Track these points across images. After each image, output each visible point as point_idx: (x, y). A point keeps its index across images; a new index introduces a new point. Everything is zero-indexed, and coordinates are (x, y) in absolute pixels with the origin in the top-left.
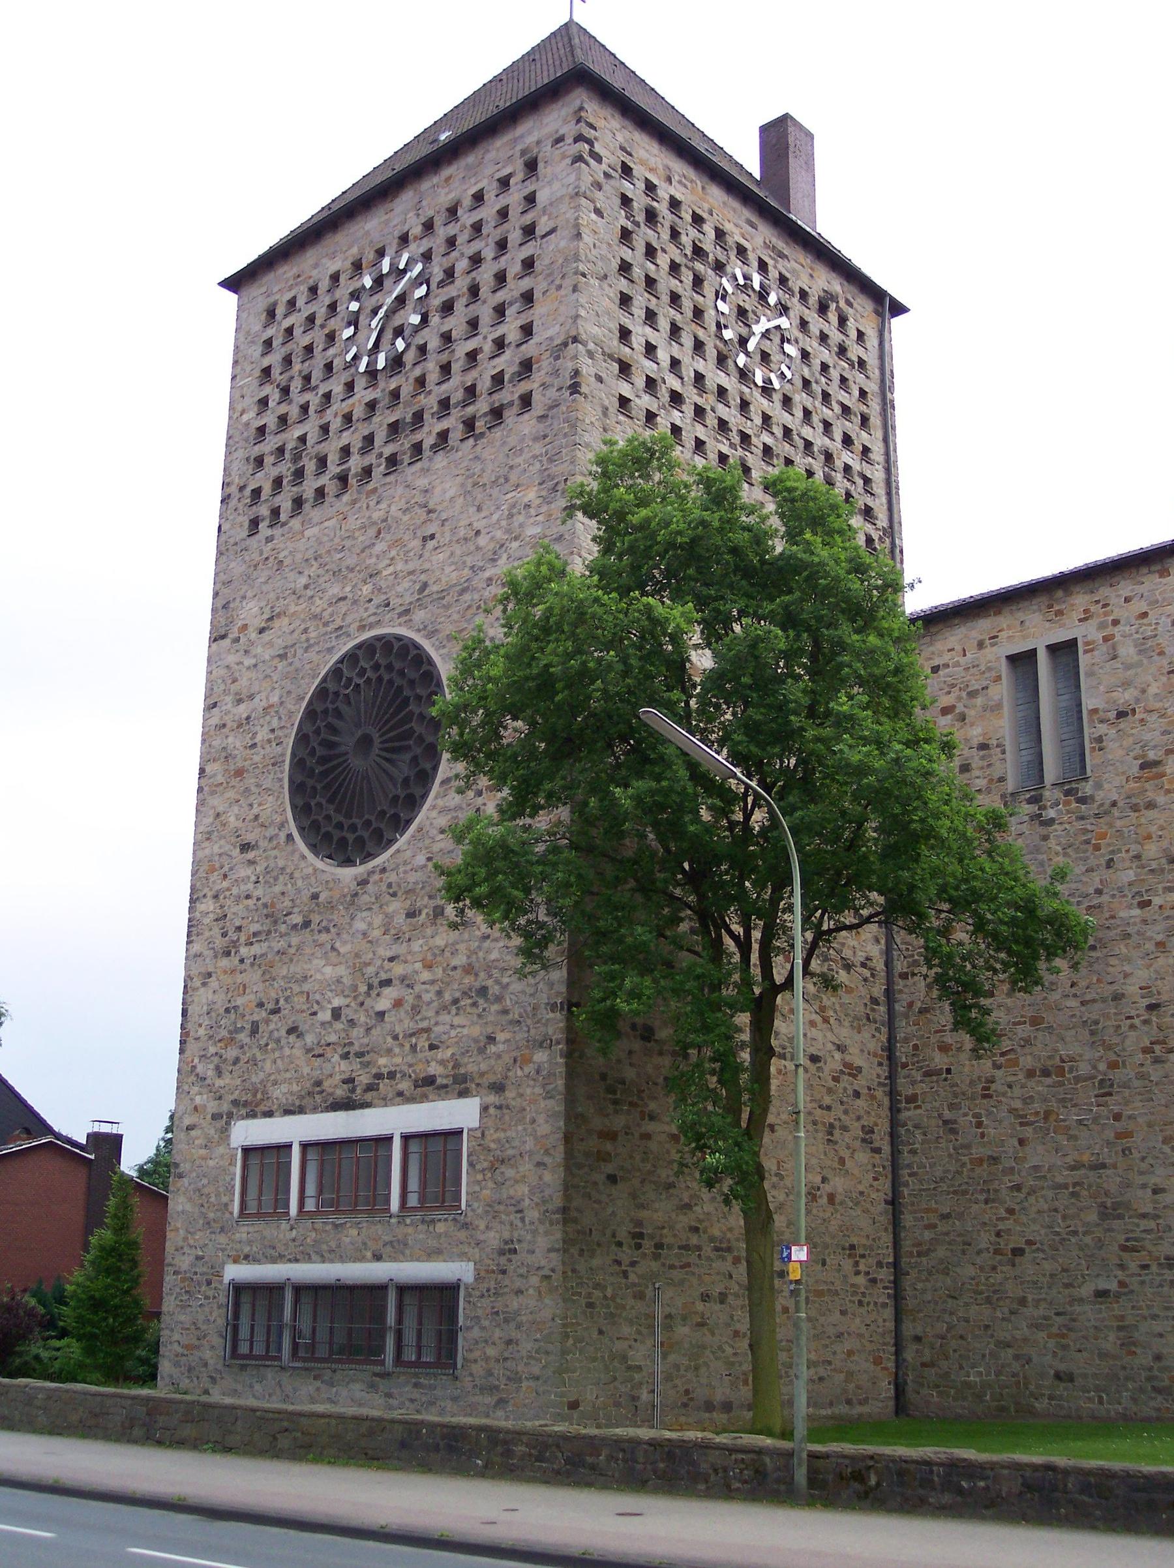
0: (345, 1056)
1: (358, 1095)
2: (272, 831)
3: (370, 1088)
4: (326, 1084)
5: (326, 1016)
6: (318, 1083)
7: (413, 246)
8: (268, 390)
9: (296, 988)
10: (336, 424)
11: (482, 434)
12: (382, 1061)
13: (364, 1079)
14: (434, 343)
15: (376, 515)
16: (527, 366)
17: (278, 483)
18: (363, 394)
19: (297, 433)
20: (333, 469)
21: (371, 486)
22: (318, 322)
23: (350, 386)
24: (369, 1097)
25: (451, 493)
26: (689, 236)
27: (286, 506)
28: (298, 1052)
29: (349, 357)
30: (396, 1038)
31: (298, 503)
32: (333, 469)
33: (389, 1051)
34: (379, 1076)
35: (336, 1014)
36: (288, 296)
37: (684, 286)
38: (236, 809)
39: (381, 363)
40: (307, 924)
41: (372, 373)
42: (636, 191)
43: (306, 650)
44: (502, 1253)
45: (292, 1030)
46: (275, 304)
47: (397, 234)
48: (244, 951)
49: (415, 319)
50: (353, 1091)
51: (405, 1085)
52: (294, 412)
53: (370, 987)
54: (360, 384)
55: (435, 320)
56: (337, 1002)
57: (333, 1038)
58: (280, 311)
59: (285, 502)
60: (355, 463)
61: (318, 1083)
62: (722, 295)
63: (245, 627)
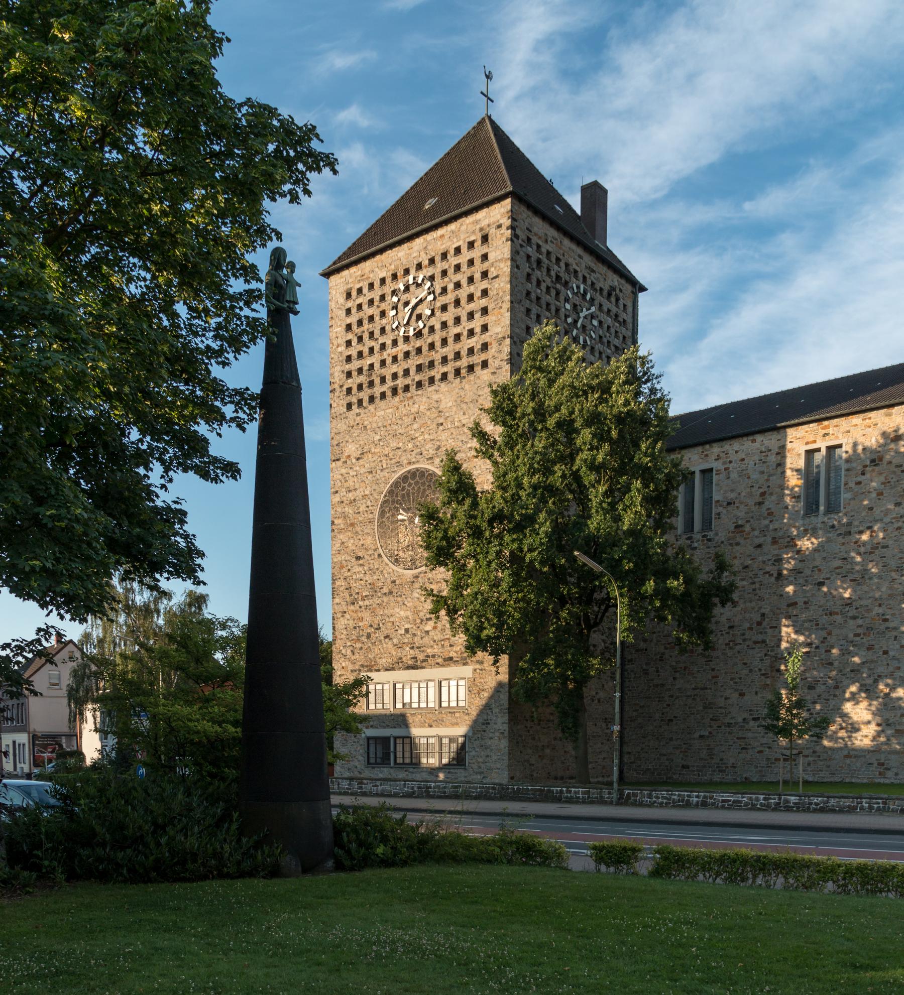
0: (412, 648)
1: (419, 663)
2: (370, 552)
3: (424, 661)
4: (404, 659)
5: (403, 632)
7: (425, 271)
8: (350, 336)
9: (387, 620)
10: (389, 361)
11: (464, 377)
12: (429, 651)
13: (421, 657)
14: (438, 327)
15: (414, 409)
16: (485, 347)
17: (360, 387)
18: (402, 347)
19: (369, 362)
20: (390, 383)
21: (409, 395)
22: (376, 303)
23: (395, 343)
24: (424, 664)
25: (450, 404)
27: (366, 399)
29: (394, 327)
30: (435, 641)
31: (372, 399)
32: (390, 383)
33: (432, 647)
34: (428, 656)
35: (407, 631)
36: (358, 286)
38: (352, 541)
39: (411, 333)
40: (391, 593)
41: (407, 339)
43: (382, 470)
44: (483, 724)
46: (351, 289)
47: (416, 263)
48: (361, 603)
49: (428, 312)
50: (417, 662)
52: (366, 351)
53: (422, 620)
54: (400, 341)
55: (438, 313)
56: (407, 626)
57: (406, 641)
58: (354, 293)
59: (364, 395)
60: (401, 382)
63: (349, 456)
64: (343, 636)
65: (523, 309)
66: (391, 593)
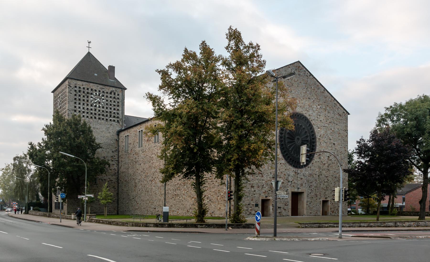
26: (86, 91)
37: (86, 98)
42: (77, 89)
62: (92, 97)
65: (74, 103)
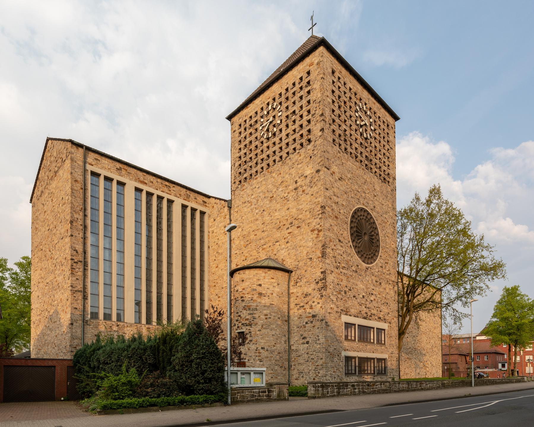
3: (371, 316)
4: (362, 312)
6: (360, 312)
13: (369, 314)
24: (370, 318)
28: (356, 303)
35: (363, 297)
45: (354, 297)
51: (376, 318)
56: (364, 294)
57: (363, 302)
61: (360, 312)
64: (331, 287)
66: (356, 272)
